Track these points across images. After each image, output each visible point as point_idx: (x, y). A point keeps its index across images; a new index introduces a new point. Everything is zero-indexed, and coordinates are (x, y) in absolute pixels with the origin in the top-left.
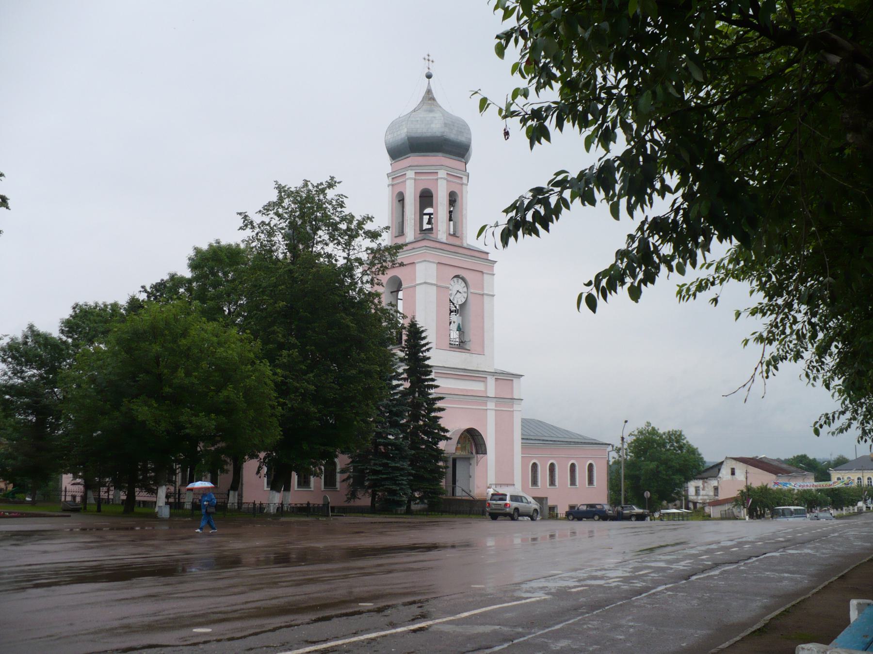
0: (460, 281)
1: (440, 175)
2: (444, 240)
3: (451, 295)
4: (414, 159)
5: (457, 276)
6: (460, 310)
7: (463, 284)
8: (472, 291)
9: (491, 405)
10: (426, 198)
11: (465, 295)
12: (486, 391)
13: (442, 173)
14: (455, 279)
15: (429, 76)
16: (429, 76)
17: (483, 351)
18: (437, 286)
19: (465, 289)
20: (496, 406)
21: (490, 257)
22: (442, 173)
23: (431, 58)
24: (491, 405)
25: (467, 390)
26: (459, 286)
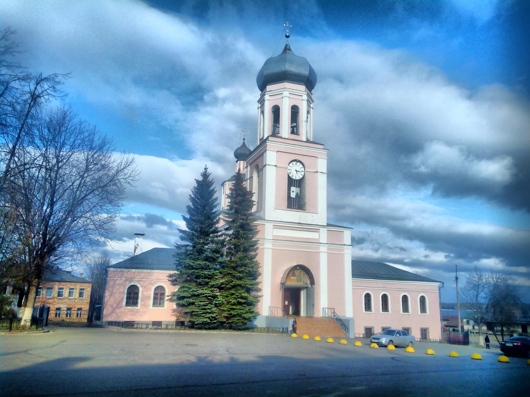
0: (298, 163)
1: (284, 95)
2: (287, 137)
4: (269, 88)
6: (299, 183)
7: (301, 166)
10: (276, 111)
11: (303, 173)
12: (319, 239)
13: (286, 93)
14: (294, 163)
19: (303, 169)
24: (323, 249)
25: (297, 238)
26: (299, 167)
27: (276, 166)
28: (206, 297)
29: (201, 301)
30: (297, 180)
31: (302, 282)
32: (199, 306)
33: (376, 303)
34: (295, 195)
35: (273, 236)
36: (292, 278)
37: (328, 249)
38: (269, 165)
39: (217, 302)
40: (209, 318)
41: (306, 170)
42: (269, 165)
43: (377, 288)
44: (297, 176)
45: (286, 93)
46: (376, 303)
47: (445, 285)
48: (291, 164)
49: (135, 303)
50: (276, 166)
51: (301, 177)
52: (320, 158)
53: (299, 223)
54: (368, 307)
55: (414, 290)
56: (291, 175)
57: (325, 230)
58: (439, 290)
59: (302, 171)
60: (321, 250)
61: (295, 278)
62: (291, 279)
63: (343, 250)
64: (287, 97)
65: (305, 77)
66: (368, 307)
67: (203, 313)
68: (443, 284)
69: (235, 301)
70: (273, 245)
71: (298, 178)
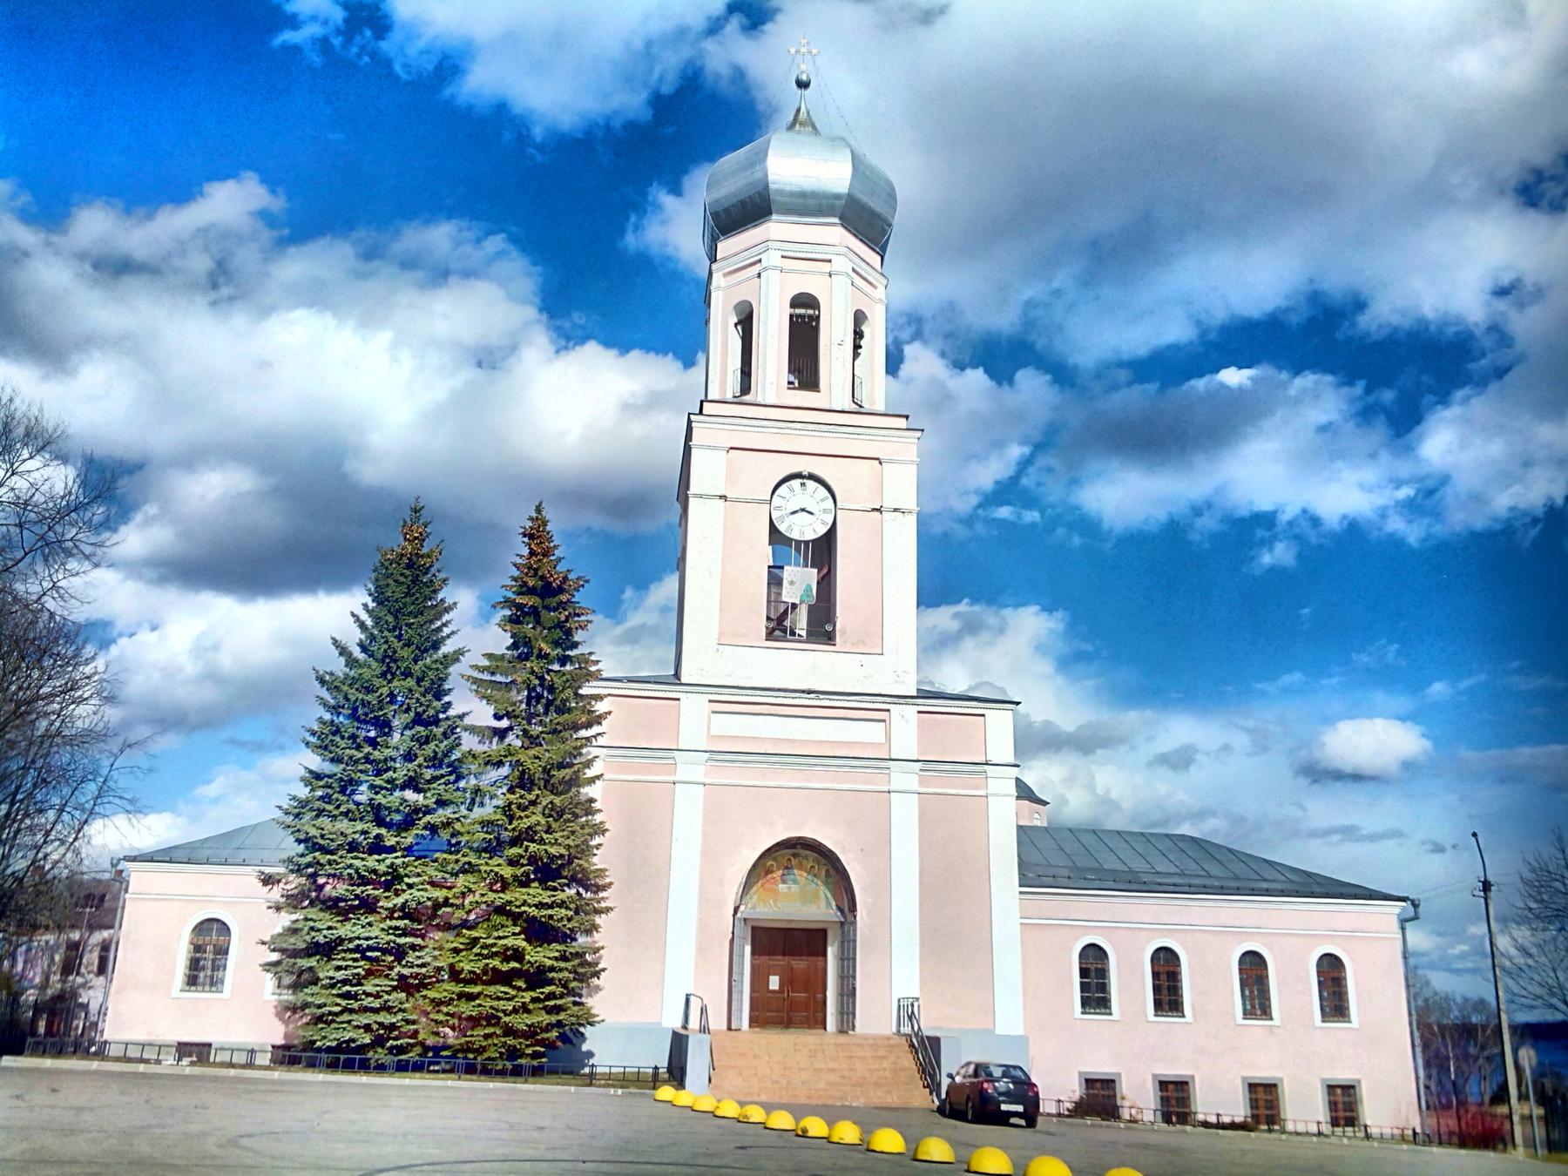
0: (811, 484)
1: (764, 264)
13: (772, 258)
14: (796, 483)
24: (904, 779)
27: (723, 497)
28: (357, 949)
29: (339, 968)
30: (807, 543)
32: (333, 986)
33: (1131, 983)
35: (710, 737)
37: (921, 783)
38: (701, 496)
39: (406, 971)
40: (367, 1028)
42: (701, 496)
43: (1132, 927)
44: (807, 529)
46: (1131, 983)
47: (1421, 909)
48: (783, 490)
49: (215, 983)
50: (723, 497)
52: (890, 461)
53: (810, 692)
54: (1095, 994)
55: (1292, 933)
56: (782, 528)
57: (910, 711)
58: (1403, 929)
60: (892, 788)
61: (794, 888)
62: (776, 891)
64: (774, 268)
65: (837, 196)
66: (1095, 994)
67: (345, 1010)
68: (1415, 905)
69: (477, 967)
71: (810, 535)
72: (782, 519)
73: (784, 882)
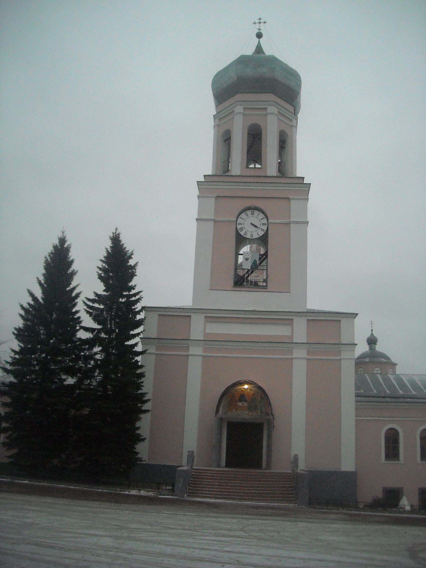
0: (256, 213)
2: (239, 174)
3: (242, 229)
5: (249, 208)
7: (261, 216)
8: (273, 221)
9: (300, 353)
11: (265, 228)
12: (292, 336)
14: (249, 212)
15: (259, 36)
16: (259, 36)
17: (289, 289)
18: (215, 222)
19: (265, 221)
20: (308, 355)
21: (305, 182)
22: (239, 109)
23: (261, 21)
24: (300, 353)
26: (257, 218)
31: (259, 412)
34: (250, 264)
35: (205, 334)
36: (240, 404)
37: (309, 353)
41: (270, 221)
45: (239, 109)
48: (243, 215)
51: (261, 233)
52: (294, 199)
56: (242, 233)
59: (263, 224)
60: (294, 356)
61: (245, 404)
63: (339, 353)
64: (240, 113)
70: (205, 350)
72: (242, 229)
73: (241, 401)
